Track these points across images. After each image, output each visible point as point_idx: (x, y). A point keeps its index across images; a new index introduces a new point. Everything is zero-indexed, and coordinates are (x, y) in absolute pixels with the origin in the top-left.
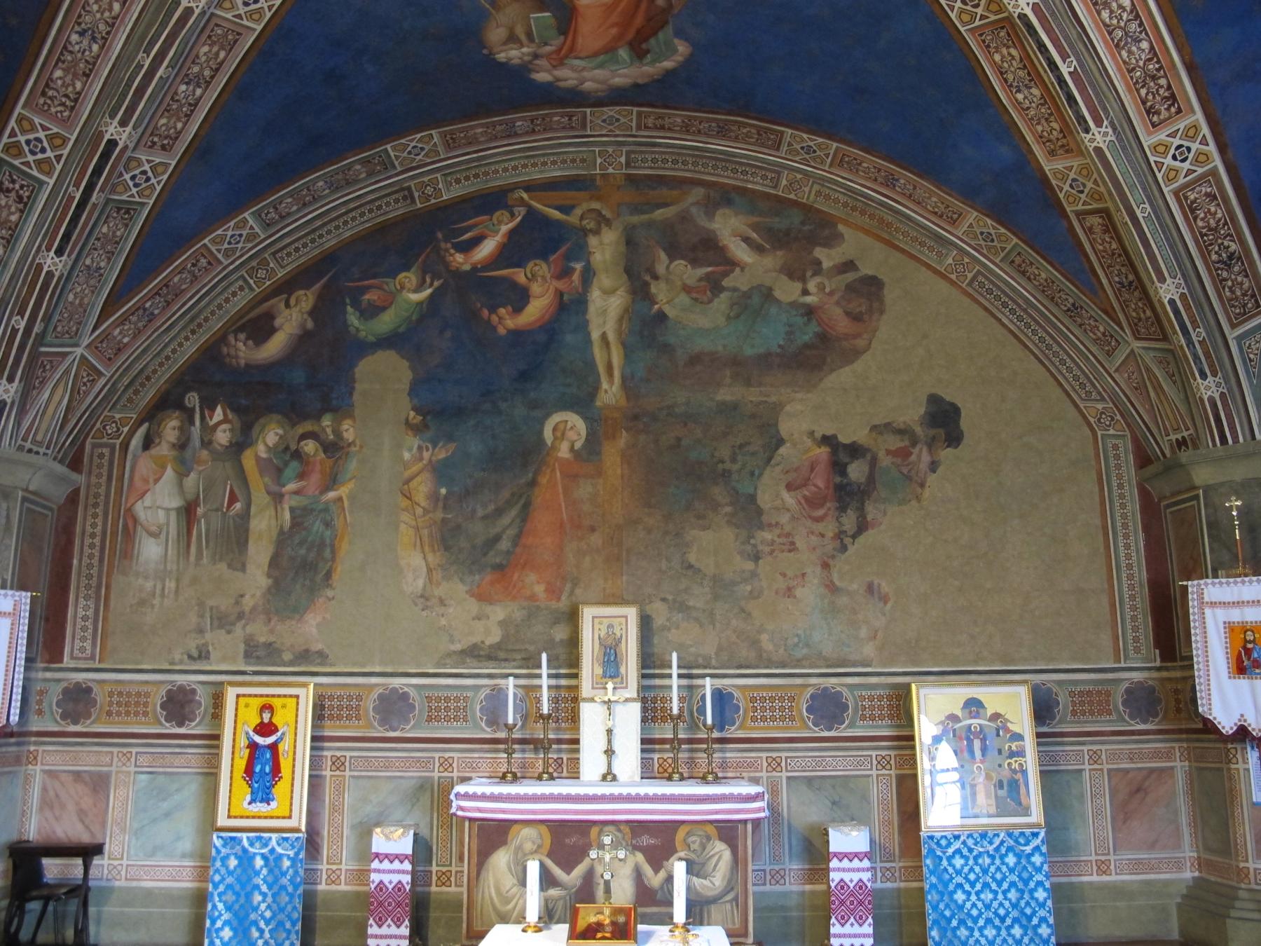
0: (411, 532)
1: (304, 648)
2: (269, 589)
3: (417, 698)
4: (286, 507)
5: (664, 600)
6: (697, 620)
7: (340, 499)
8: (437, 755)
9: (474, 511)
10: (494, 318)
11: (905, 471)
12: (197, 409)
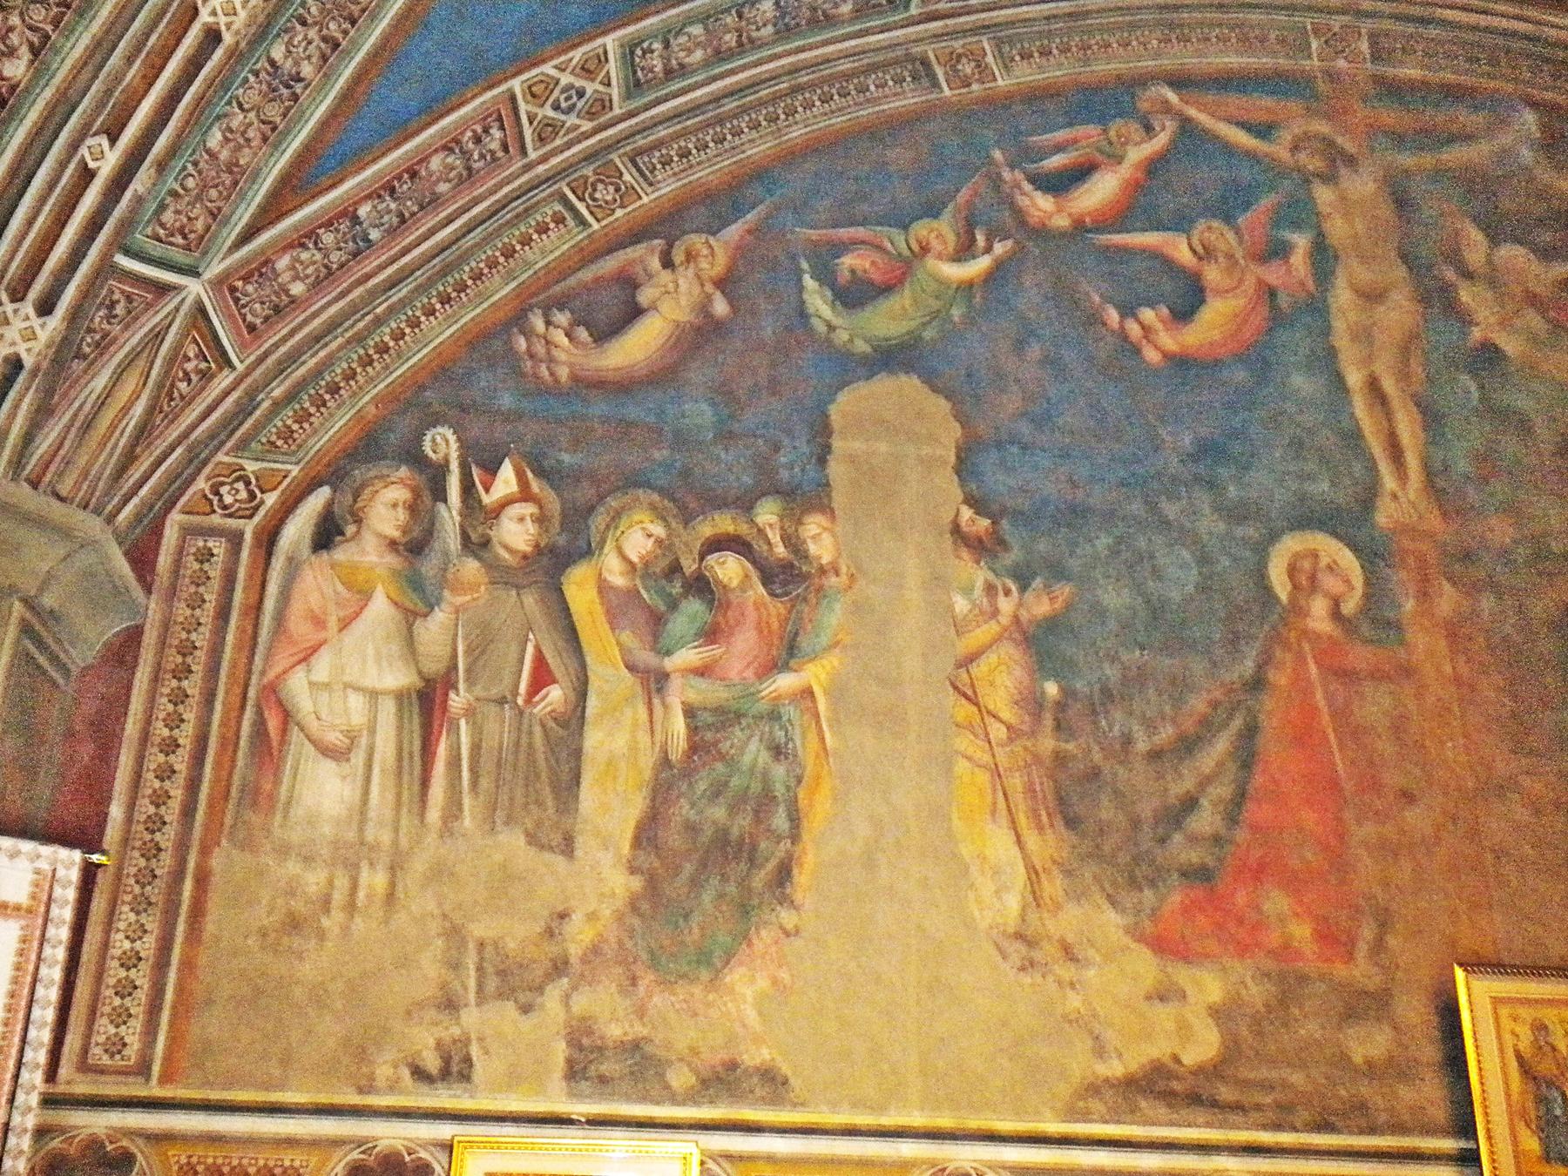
0: (983, 778)
1: (723, 1055)
2: (634, 905)
9: (1127, 741)
12: (454, 466)
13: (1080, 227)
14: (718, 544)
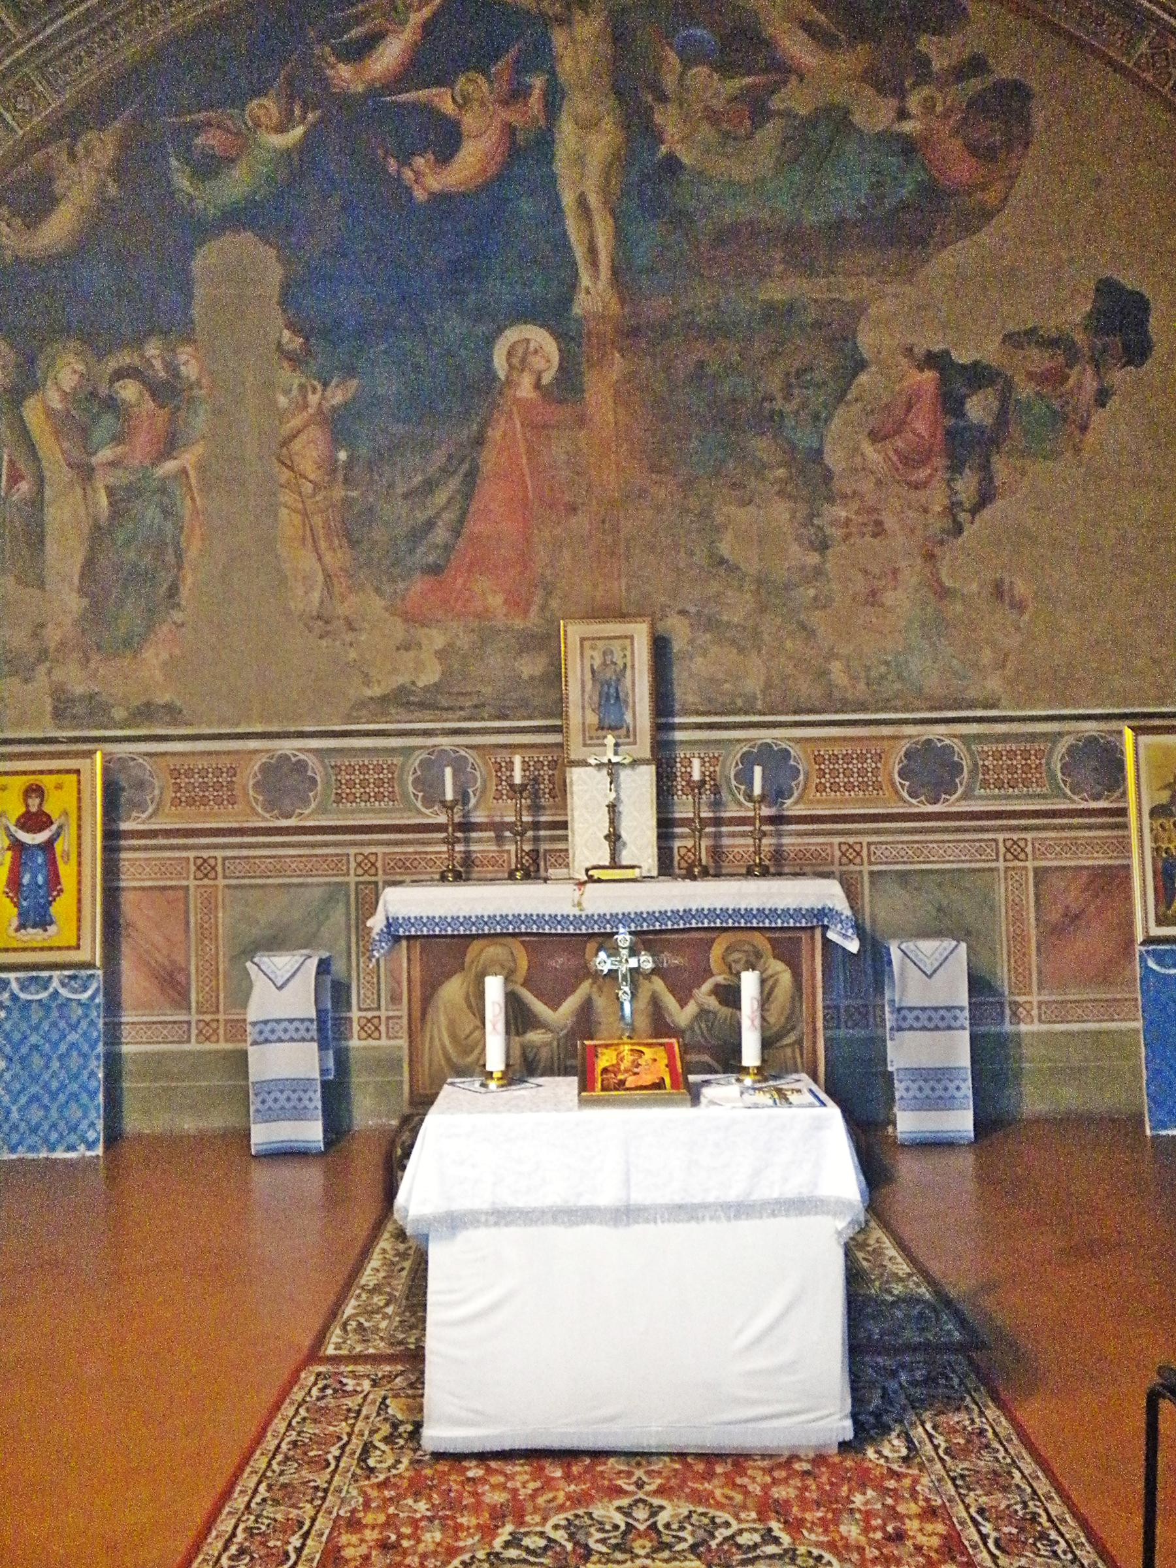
0: (297, 519)
1: (144, 699)
2: (83, 617)
3: (319, 768)
4: (100, 485)
5: (683, 612)
6: (733, 642)
7: (184, 471)
8: (352, 851)
10: (408, 174)
11: (1057, 407)
13: (373, 92)
14: (120, 374)
